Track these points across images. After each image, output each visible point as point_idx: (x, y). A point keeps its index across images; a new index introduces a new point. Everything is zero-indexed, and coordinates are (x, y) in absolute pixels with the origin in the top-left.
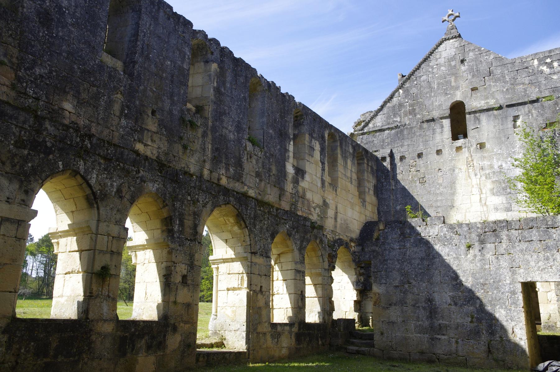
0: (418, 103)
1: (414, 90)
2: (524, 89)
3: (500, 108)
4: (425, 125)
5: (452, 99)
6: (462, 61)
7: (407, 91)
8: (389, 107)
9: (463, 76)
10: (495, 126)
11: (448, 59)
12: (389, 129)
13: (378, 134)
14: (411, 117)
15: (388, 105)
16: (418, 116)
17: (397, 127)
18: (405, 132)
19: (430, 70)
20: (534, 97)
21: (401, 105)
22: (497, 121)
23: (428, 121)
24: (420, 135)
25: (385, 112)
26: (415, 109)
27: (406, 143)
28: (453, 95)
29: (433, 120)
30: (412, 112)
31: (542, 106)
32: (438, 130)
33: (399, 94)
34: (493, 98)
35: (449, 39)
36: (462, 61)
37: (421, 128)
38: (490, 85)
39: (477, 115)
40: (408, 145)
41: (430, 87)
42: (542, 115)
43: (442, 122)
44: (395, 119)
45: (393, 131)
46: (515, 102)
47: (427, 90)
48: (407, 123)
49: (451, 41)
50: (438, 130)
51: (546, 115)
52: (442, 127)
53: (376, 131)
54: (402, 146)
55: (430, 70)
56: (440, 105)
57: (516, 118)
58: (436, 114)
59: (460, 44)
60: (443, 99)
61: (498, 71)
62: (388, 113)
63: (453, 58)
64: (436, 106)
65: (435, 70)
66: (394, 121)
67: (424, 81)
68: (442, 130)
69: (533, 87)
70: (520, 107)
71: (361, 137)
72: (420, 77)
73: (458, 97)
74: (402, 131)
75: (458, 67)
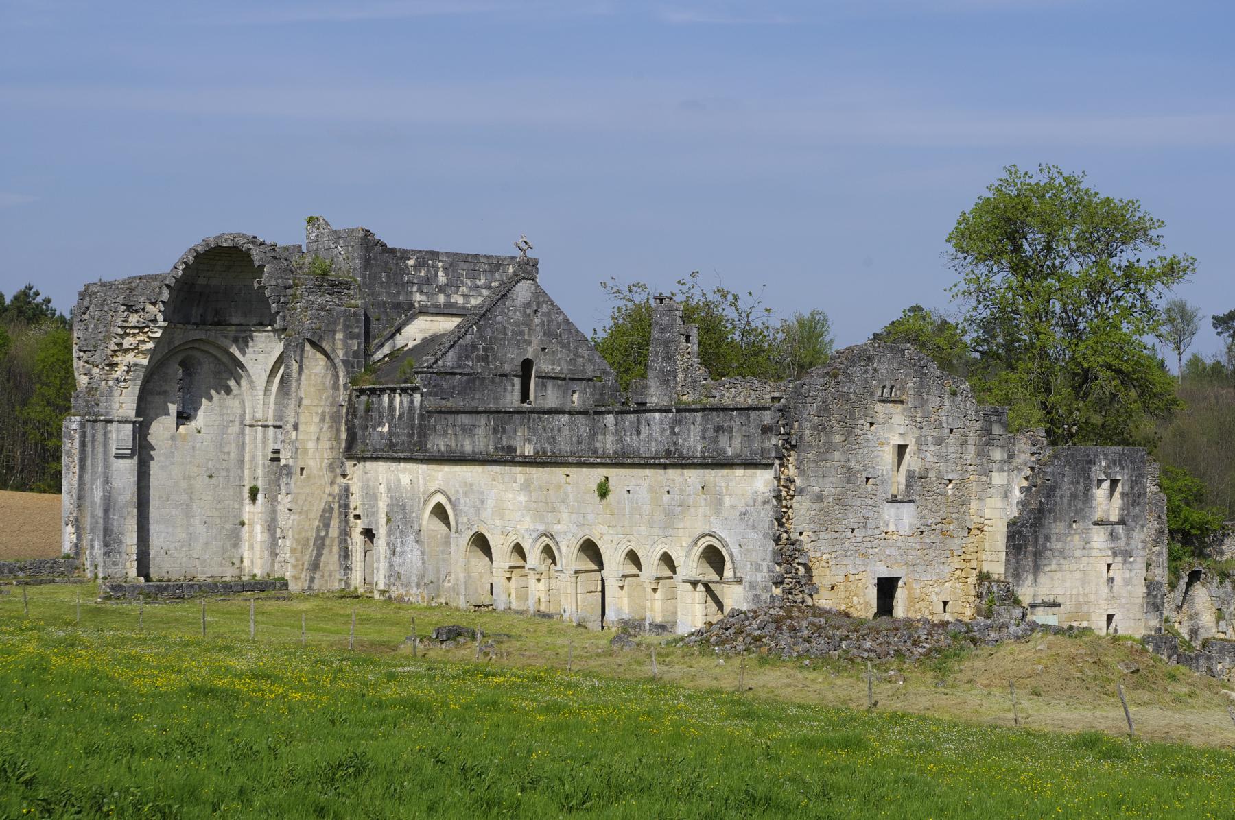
1: (489, 332)
4: (497, 379)
6: (536, 311)
7: (479, 329)
12: (461, 374)
17: (469, 374)
20: (589, 374)
21: (474, 347)
30: (485, 359)
32: (509, 388)
36: (536, 311)
37: (493, 381)
41: (505, 334)
47: (501, 336)
50: (509, 388)
52: (513, 386)
53: (447, 374)
54: (473, 399)
56: (512, 357)
57: (574, 392)
58: (507, 368)
62: (459, 352)
63: (528, 305)
72: (496, 316)
73: (529, 355)
74: (474, 380)
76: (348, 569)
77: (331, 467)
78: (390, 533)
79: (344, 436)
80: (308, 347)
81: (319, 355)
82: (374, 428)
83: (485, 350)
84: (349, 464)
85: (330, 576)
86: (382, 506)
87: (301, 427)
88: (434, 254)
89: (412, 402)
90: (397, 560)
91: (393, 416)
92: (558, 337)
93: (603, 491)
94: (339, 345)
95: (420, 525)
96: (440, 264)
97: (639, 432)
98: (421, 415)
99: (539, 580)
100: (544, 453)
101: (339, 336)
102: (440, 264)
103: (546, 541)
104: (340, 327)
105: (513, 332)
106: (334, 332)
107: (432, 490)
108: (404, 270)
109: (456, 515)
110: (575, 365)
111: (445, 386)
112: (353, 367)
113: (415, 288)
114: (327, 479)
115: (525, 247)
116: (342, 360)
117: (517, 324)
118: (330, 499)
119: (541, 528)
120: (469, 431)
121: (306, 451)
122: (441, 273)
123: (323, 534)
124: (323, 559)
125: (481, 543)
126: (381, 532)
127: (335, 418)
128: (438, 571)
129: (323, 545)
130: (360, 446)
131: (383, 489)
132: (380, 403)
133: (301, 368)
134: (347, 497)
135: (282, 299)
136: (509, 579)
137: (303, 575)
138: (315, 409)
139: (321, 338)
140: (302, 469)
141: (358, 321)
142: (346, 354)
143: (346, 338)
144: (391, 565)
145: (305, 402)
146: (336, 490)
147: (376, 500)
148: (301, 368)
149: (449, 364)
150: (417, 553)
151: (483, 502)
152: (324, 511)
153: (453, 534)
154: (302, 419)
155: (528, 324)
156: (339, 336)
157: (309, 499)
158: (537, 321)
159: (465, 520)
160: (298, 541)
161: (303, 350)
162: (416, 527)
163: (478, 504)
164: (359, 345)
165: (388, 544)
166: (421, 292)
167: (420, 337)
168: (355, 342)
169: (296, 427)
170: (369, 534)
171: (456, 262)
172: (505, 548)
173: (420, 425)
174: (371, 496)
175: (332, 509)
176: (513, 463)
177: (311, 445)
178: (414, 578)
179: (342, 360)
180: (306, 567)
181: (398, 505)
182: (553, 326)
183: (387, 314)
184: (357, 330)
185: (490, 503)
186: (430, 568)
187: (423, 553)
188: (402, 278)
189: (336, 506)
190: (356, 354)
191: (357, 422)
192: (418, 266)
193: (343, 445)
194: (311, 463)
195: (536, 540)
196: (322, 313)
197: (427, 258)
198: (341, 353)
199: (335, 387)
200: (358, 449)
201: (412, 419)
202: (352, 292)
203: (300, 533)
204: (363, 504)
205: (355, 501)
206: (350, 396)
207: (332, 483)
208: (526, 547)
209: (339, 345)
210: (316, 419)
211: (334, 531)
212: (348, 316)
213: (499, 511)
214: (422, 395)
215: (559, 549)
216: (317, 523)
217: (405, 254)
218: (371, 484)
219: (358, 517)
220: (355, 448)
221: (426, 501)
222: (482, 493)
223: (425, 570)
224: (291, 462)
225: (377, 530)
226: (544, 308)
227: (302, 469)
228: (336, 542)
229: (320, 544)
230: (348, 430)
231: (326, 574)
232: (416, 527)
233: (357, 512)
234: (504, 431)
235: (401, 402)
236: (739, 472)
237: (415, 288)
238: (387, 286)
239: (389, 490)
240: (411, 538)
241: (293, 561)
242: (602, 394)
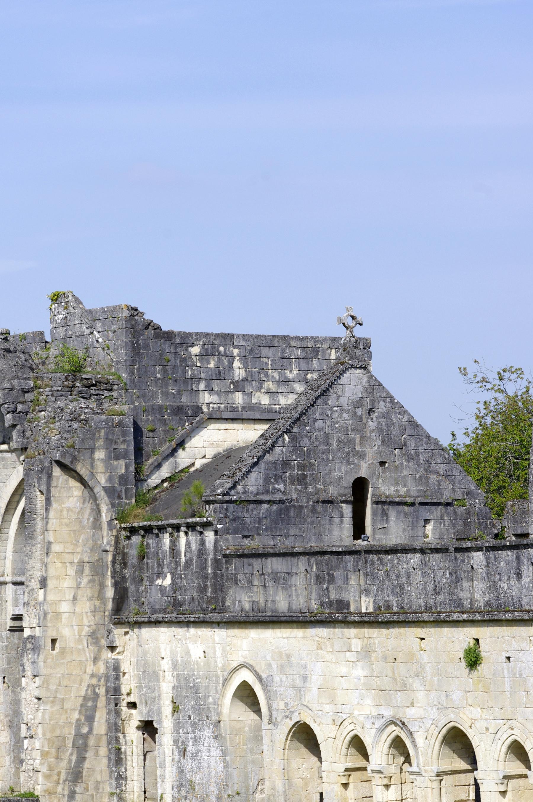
0: (311, 465)
1: (305, 443)
2: (438, 481)
3: (413, 504)
4: (320, 508)
5: (356, 472)
6: (370, 411)
7: (293, 439)
8: (268, 462)
9: (370, 438)
10: (404, 530)
11: (353, 402)
12: (269, 502)
13: (252, 506)
14: (299, 487)
15: (267, 456)
16: (310, 489)
18: (292, 513)
19: (329, 412)
20: (447, 496)
21: (286, 464)
22: (407, 522)
23: (324, 502)
24: (312, 522)
25: (262, 470)
26: (306, 476)
27: (292, 533)
28: (358, 466)
29: (331, 502)
30: (301, 480)
31: (455, 512)
33: (284, 440)
34: (405, 485)
35: (356, 368)
36: (370, 411)
38: (402, 464)
39: (386, 507)
40: (295, 536)
41: (328, 444)
42: (454, 525)
43: (342, 507)
44: (277, 486)
45: (275, 507)
46: (430, 501)
47: (322, 447)
48: (294, 497)
49: (358, 371)
50: (337, 520)
51: (458, 527)
52: (342, 516)
53: (249, 502)
54: (287, 535)
55: (329, 412)
57: (427, 521)
58: (333, 492)
59: (369, 381)
60: (344, 469)
61: (412, 445)
62: (266, 471)
63: (358, 403)
64: (334, 478)
65: (335, 416)
66: (275, 489)
67: (319, 430)
68: (342, 521)
69: (447, 482)
70: (433, 508)
71: (225, 505)
72: (315, 420)
74: (288, 509)
75: (364, 421)
76: (121, 778)
77: (94, 636)
78: (178, 726)
79: (110, 593)
80: (57, 471)
81: (74, 484)
82: (152, 581)
83: (301, 467)
84: (118, 632)
85: (97, 788)
86: (166, 689)
87: (50, 583)
88: (227, 338)
89: (202, 543)
90: (188, 764)
91: (177, 564)
92: (402, 446)
93: (473, 660)
94: (100, 467)
95: (219, 714)
96: (236, 352)
97: (519, 576)
98: (216, 561)
99: (387, 786)
100: (388, 607)
101: (100, 455)
102: (236, 352)
103: (396, 731)
104: (101, 442)
105: (339, 441)
106: (92, 450)
107: (235, 664)
108: (185, 362)
109: (268, 698)
110: (427, 484)
111: (248, 520)
112: (119, 497)
113: (202, 386)
114: (89, 654)
115: (351, 323)
116: (105, 489)
117: (344, 430)
118: (94, 681)
119: (388, 713)
120: (283, 580)
121: (58, 615)
122: (237, 364)
123: (85, 730)
124: (87, 765)
125: (306, 737)
126: (166, 725)
127: (97, 568)
128: (246, 777)
129: (86, 745)
130: (132, 606)
131: (166, 665)
132: (159, 547)
133: (48, 501)
134: (117, 678)
135: (20, 407)
136: (345, 786)
137: (59, 789)
138: (68, 558)
139: (75, 459)
140: (54, 641)
141: (125, 434)
142: (110, 479)
143: (109, 457)
144: (181, 771)
145: (56, 548)
146: (101, 668)
147: (158, 680)
148: (48, 501)
149: (252, 489)
150: (216, 753)
151: (305, 679)
152: (86, 698)
153: (265, 725)
154: (52, 571)
155: (360, 430)
156: (100, 455)
157: (65, 682)
158: (372, 425)
159: (282, 706)
160: (50, 740)
161: (50, 476)
162: (214, 718)
163: (299, 682)
164: (127, 466)
165: (176, 742)
166: (211, 391)
167: (211, 453)
168: (122, 462)
169: (43, 583)
170: (149, 728)
171: (256, 347)
172: (339, 742)
173: (215, 574)
174: (150, 675)
175: (97, 696)
176: (346, 623)
177: (65, 607)
179: (105, 489)
180: (63, 777)
181: (187, 687)
182: (395, 432)
183: (164, 423)
184: (123, 447)
185: (315, 681)
186: (235, 773)
187: (224, 753)
188: (184, 373)
189: (102, 691)
190: (123, 479)
191: (128, 573)
192: (205, 355)
193: (110, 605)
194: (66, 632)
195: (381, 730)
196: (76, 425)
197: (217, 344)
198: (102, 479)
199: (96, 525)
200: (131, 610)
202: (115, 394)
203: (53, 730)
204: (140, 687)
205: (128, 683)
206: (117, 538)
207: (96, 660)
208: (368, 741)
209: (100, 467)
210: (71, 571)
211: (100, 726)
212: (111, 427)
213: (328, 690)
214: (216, 532)
215: (414, 742)
216: (76, 716)
217: (187, 340)
218: (149, 658)
219: (133, 705)
220: (125, 610)
221: (226, 681)
222: (304, 667)
223: (229, 775)
224: (38, 632)
225: (160, 722)
226: (382, 407)
227: (54, 641)
228: (104, 741)
229: (82, 745)
230: (116, 584)
231: (91, 786)
232: (214, 718)
233: (132, 699)
234: (332, 579)
235: (188, 543)
237: (202, 386)
238: (164, 383)
239: (175, 666)
240: (208, 732)
241: (44, 769)
242: (465, 524)
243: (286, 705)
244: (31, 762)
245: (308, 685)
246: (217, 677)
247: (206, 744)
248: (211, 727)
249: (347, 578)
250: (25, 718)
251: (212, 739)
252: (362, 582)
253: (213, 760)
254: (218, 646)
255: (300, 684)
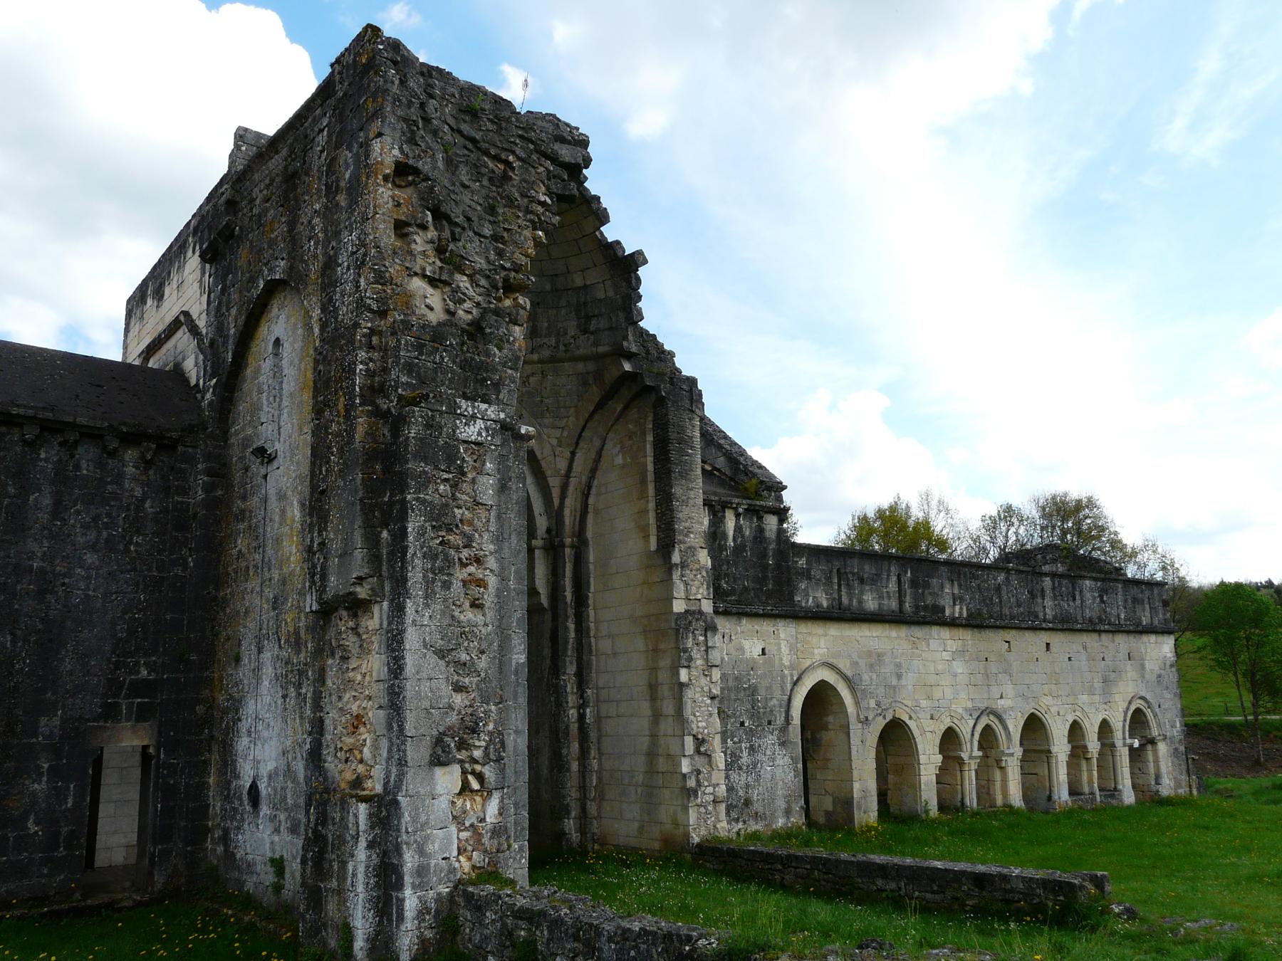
89: (761, 530)
97: (1074, 599)
100: (980, 614)
151: (899, 676)
159: (872, 704)
173: (778, 566)
178: (781, 804)
181: (738, 689)
201: (763, 555)
215: (1006, 728)
222: (899, 666)
234: (927, 585)
235: (738, 529)
236: (1153, 638)
240: (770, 740)
243: (878, 704)
244: (710, 790)
245: (903, 682)
246: (783, 677)
247: (768, 753)
248: (776, 732)
249: (942, 587)
250: (694, 726)
251: (777, 747)
252: (956, 591)
253: (779, 772)
254: (783, 644)
255: (894, 682)
